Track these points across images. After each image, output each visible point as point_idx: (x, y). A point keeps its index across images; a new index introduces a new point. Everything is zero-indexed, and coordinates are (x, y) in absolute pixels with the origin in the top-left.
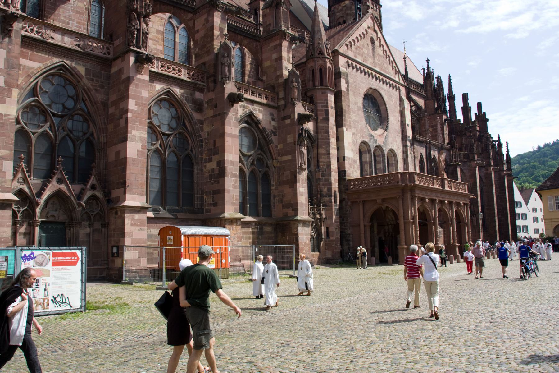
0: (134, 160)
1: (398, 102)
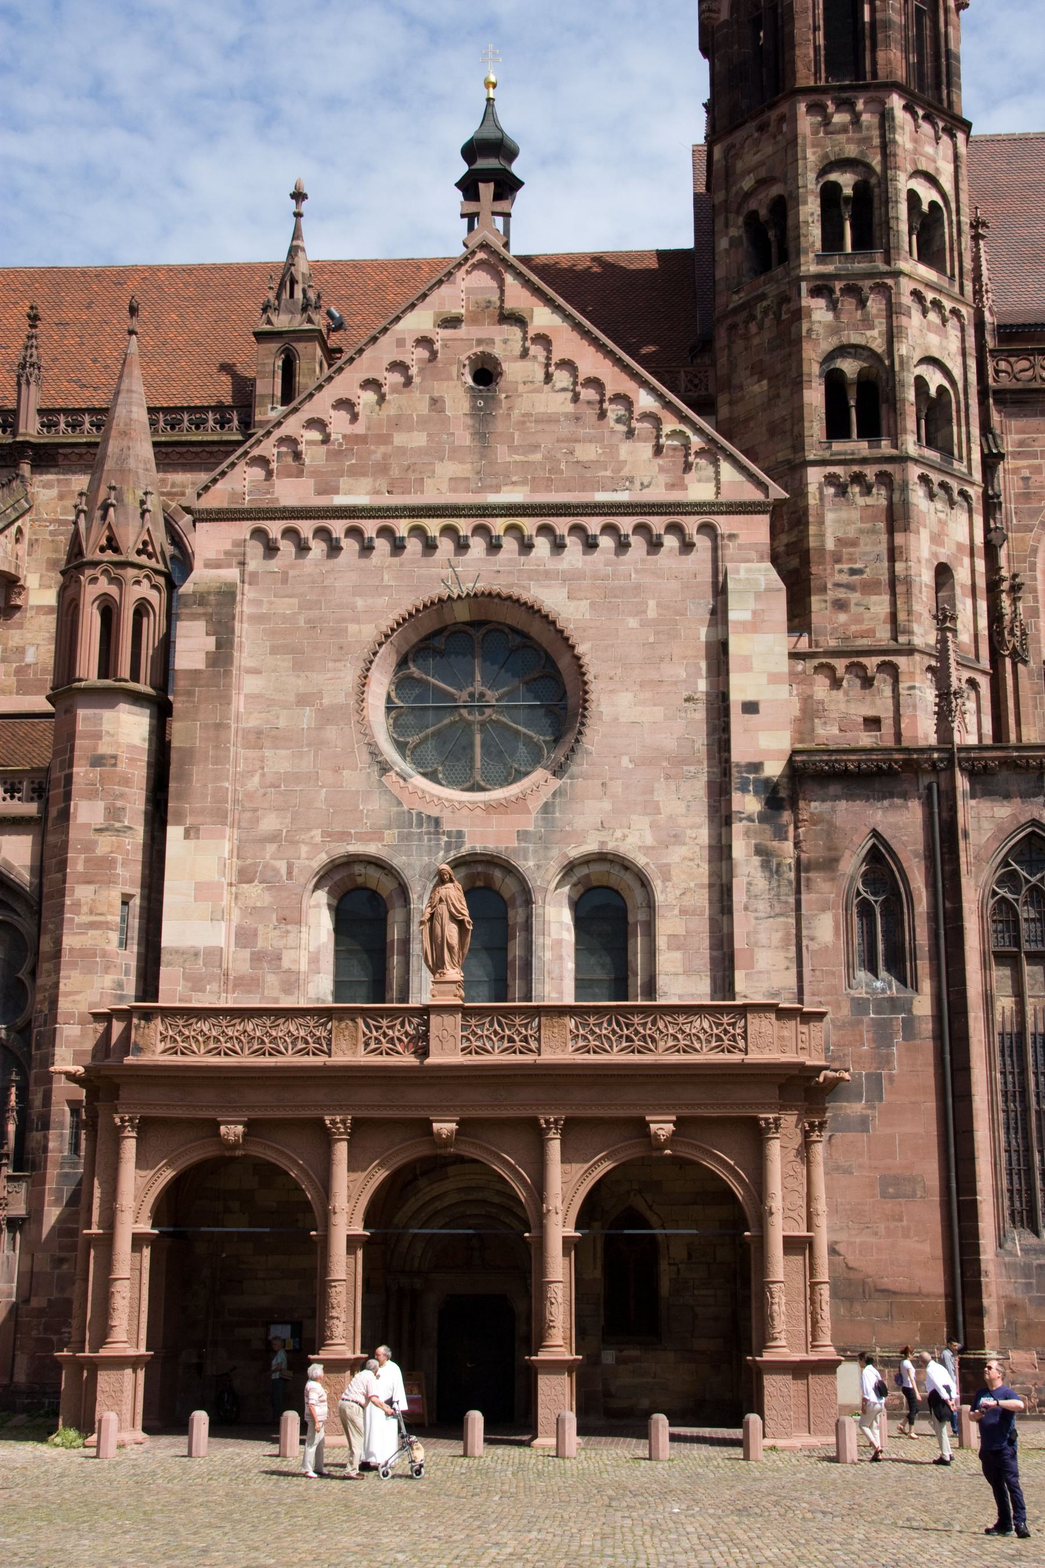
1: (708, 602)
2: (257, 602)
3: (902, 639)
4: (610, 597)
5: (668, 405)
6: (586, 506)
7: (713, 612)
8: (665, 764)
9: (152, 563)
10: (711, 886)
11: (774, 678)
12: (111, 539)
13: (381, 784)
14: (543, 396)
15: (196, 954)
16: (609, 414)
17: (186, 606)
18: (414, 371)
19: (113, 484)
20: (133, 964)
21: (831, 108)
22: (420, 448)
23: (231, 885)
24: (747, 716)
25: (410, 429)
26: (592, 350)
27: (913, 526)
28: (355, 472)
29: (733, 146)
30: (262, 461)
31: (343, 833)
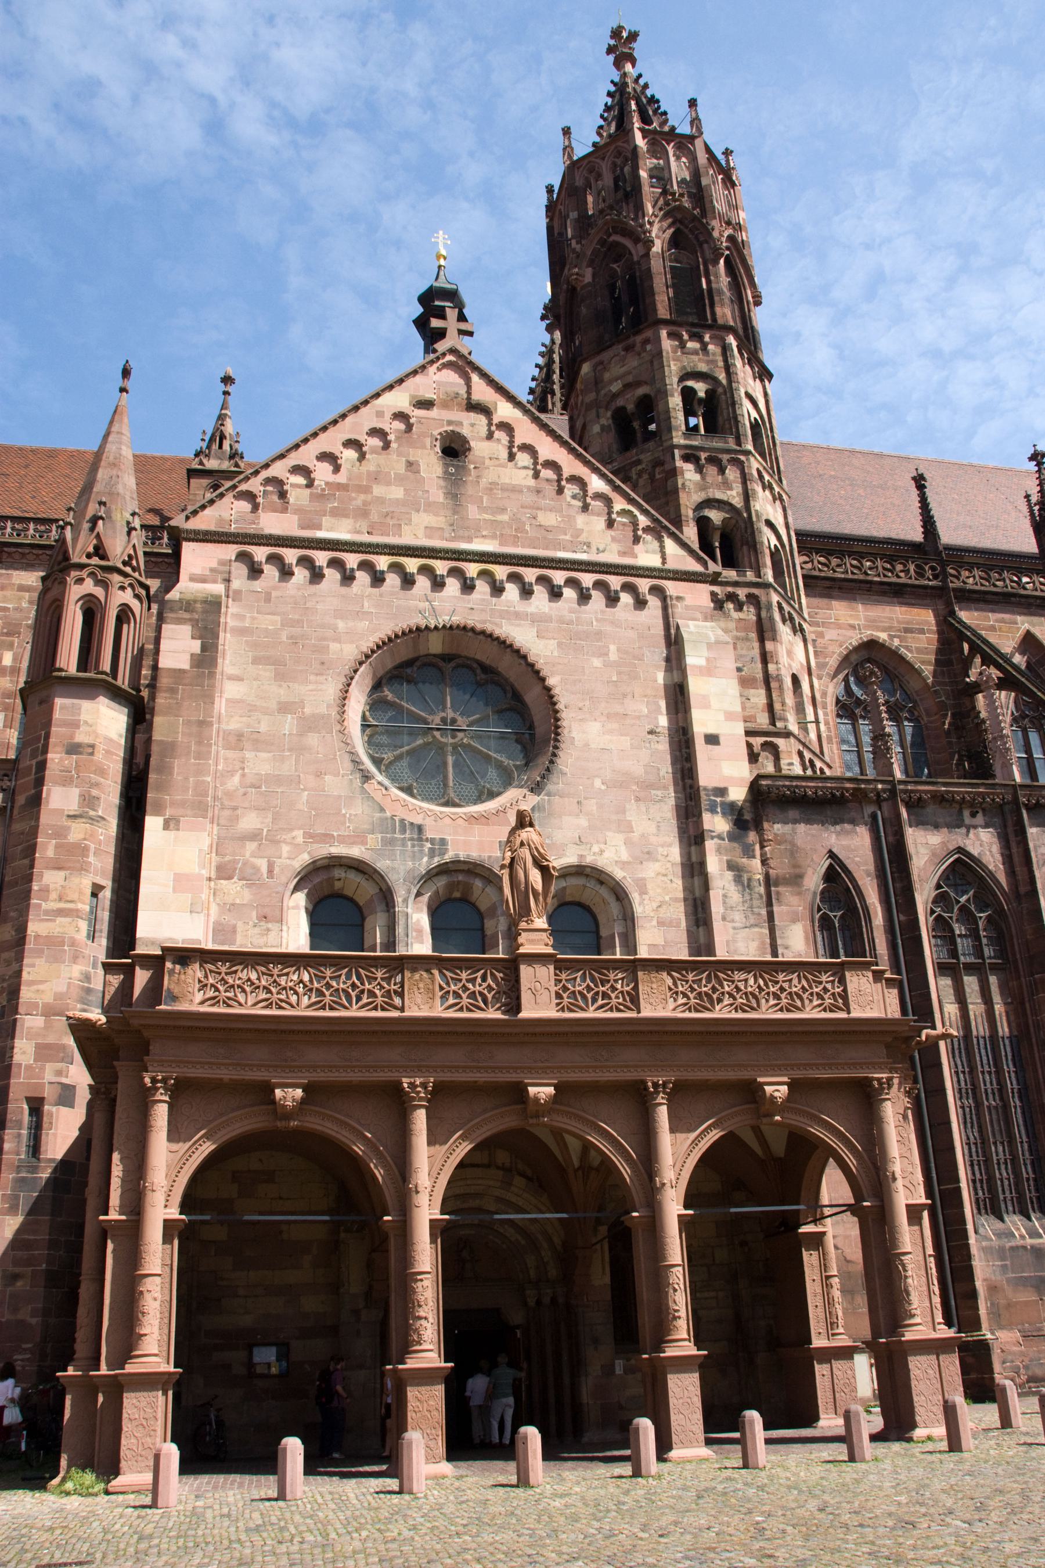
3: (779, 724)
4: (575, 639)
5: (616, 489)
6: (552, 560)
7: (668, 660)
8: (634, 788)
10: (685, 900)
11: (729, 716)
13: (364, 791)
14: (508, 471)
16: (566, 490)
17: (172, 610)
18: (391, 437)
21: (686, 337)
22: (397, 499)
23: (210, 879)
24: (710, 747)
25: (388, 483)
26: (549, 439)
27: (778, 638)
28: (336, 513)
29: (601, 363)
30: (250, 496)
31: (326, 835)
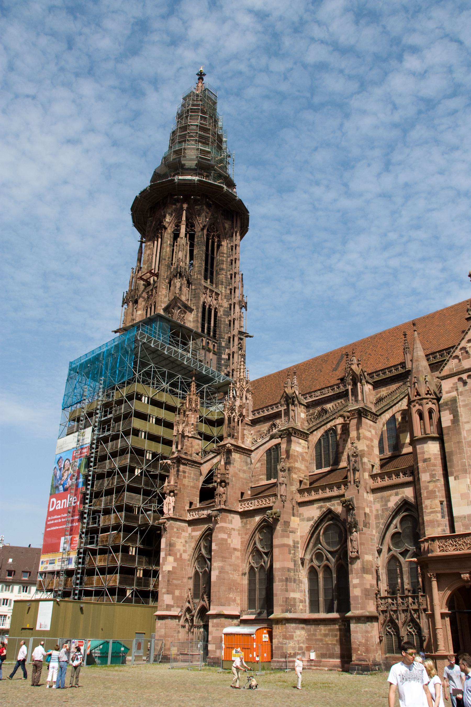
0: (214, 582)
2: (464, 401)
9: (432, 396)
12: (417, 392)
15: (465, 517)
17: (442, 407)
19: (415, 376)
20: (447, 523)
30: (457, 357)
